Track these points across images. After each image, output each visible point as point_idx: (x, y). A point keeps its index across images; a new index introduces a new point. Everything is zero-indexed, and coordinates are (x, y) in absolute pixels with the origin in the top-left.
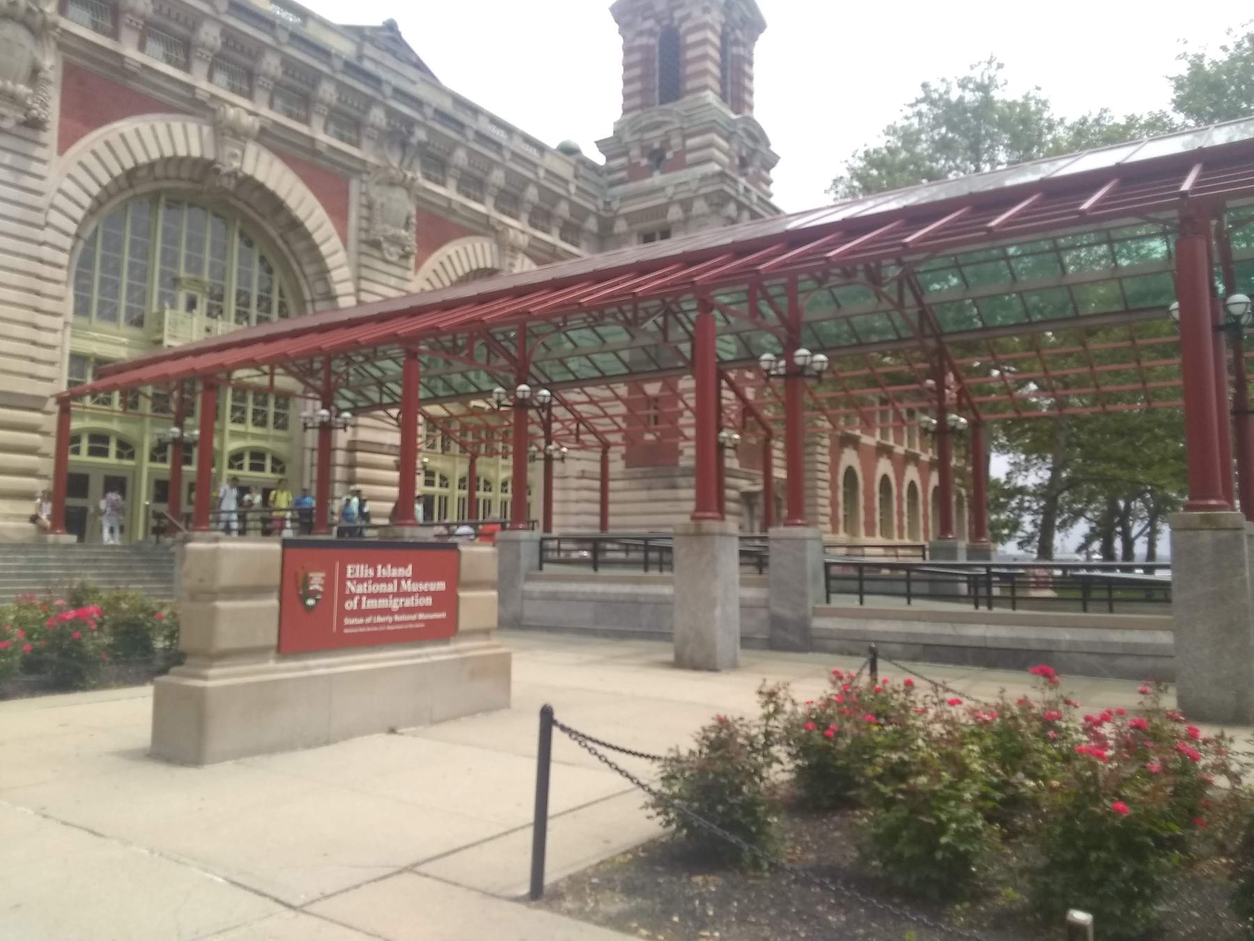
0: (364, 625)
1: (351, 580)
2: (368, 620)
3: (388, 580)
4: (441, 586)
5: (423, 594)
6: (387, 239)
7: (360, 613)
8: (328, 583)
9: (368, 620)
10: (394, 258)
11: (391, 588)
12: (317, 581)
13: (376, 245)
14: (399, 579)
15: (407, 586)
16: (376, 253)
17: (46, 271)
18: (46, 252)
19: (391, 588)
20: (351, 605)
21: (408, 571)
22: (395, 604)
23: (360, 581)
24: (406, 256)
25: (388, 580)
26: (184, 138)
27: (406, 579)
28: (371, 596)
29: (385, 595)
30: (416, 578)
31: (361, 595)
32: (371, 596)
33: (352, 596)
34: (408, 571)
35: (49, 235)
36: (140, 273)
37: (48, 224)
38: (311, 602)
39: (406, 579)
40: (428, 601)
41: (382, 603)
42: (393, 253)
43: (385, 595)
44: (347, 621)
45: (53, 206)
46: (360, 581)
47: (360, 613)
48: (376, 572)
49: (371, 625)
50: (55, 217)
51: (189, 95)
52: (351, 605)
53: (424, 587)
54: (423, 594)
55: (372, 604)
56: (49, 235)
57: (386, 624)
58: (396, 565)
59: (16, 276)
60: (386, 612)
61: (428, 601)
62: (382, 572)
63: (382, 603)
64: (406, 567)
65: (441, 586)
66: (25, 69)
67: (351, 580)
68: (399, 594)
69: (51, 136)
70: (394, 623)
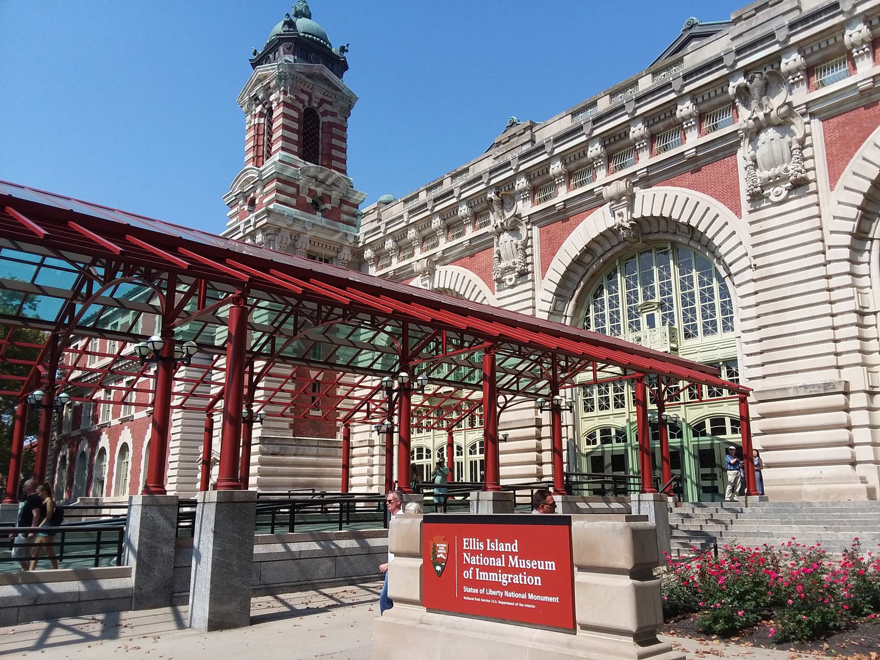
0: (478, 595)
1: (467, 551)
2: (482, 591)
3: (497, 554)
4: (551, 565)
5: (531, 572)
7: (474, 583)
8: (449, 550)
9: (482, 591)
11: (500, 563)
12: (442, 550)
14: (507, 554)
15: (514, 562)
19: (500, 563)
20: (468, 574)
21: (515, 547)
22: (504, 579)
23: (474, 553)
25: (497, 554)
27: (514, 554)
28: (483, 568)
29: (494, 569)
30: (522, 555)
31: (475, 566)
32: (483, 568)
33: (468, 566)
34: (515, 547)
38: (438, 568)
39: (514, 554)
40: (537, 581)
41: (493, 577)
43: (494, 569)
44: (467, 589)
46: (474, 553)
47: (474, 583)
48: (485, 546)
49: (485, 596)
52: (468, 574)
53: (532, 564)
54: (531, 572)
55: (483, 576)
57: (497, 597)
58: (502, 540)
60: (497, 586)
61: (537, 581)
62: (492, 546)
63: (493, 577)
64: (512, 543)
65: (551, 565)
67: (467, 551)
68: (507, 569)
70: (505, 598)
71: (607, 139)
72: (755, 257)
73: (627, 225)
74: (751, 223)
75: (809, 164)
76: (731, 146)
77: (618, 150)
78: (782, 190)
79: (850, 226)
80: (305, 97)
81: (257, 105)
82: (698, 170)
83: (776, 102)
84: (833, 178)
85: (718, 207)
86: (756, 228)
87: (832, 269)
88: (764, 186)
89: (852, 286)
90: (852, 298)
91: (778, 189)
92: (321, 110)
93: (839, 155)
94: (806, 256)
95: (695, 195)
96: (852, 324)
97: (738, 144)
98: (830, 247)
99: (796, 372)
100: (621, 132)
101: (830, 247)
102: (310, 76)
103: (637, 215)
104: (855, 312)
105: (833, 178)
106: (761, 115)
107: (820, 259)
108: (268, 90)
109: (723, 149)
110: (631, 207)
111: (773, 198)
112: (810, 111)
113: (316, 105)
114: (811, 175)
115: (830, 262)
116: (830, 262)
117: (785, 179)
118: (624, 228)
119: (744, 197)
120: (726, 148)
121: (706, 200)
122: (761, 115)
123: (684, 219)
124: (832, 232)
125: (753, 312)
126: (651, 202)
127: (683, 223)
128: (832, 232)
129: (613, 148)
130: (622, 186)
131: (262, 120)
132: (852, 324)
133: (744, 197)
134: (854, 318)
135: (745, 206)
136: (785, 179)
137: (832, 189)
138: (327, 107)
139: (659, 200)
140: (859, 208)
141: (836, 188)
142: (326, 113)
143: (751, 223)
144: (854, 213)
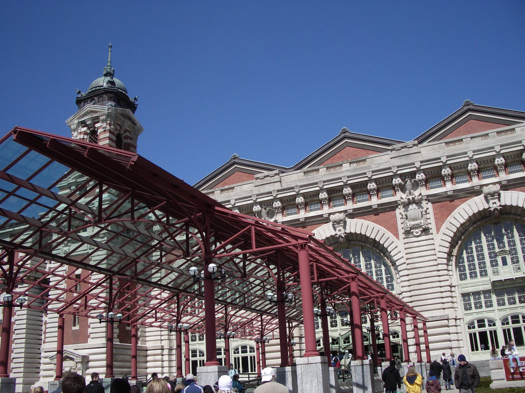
71: (330, 191)
72: (407, 259)
73: (343, 236)
74: (405, 244)
75: (429, 221)
76: (393, 207)
77: (335, 197)
78: (418, 231)
79: (447, 250)
80: (118, 128)
81: (83, 127)
82: (378, 214)
83: (416, 193)
84: (438, 230)
85: (388, 234)
86: (407, 246)
87: (440, 267)
88: (411, 228)
89: (447, 275)
90: (448, 280)
91: (417, 230)
92: (124, 135)
93: (440, 220)
94: (429, 261)
95: (377, 227)
96: (448, 291)
97: (397, 207)
98: (438, 258)
99: (427, 311)
100: (340, 189)
101: (438, 258)
102: (122, 115)
103: (348, 231)
104: (449, 286)
105: (438, 230)
106: (411, 197)
107: (435, 263)
108: (96, 120)
109: (390, 207)
110: (345, 227)
111: (414, 233)
112: (430, 198)
113: (122, 132)
114: (430, 226)
115: (439, 264)
116: (439, 264)
117: (421, 227)
118: (342, 237)
119: (401, 232)
120: (392, 207)
121: (383, 230)
122: (411, 197)
123: (373, 237)
124: (439, 252)
125: (407, 283)
126: (356, 226)
127: (372, 239)
128: (439, 252)
129: (333, 195)
130: (342, 216)
131: (86, 137)
132: (448, 291)
133: (401, 232)
134: (448, 288)
135: (402, 236)
136: (421, 227)
137: (438, 233)
138: (128, 134)
139: (358, 227)
140: (449, 243)
141: (440, 232)
142: (127, 137)
143: (405, 244)
144: (448, 245)
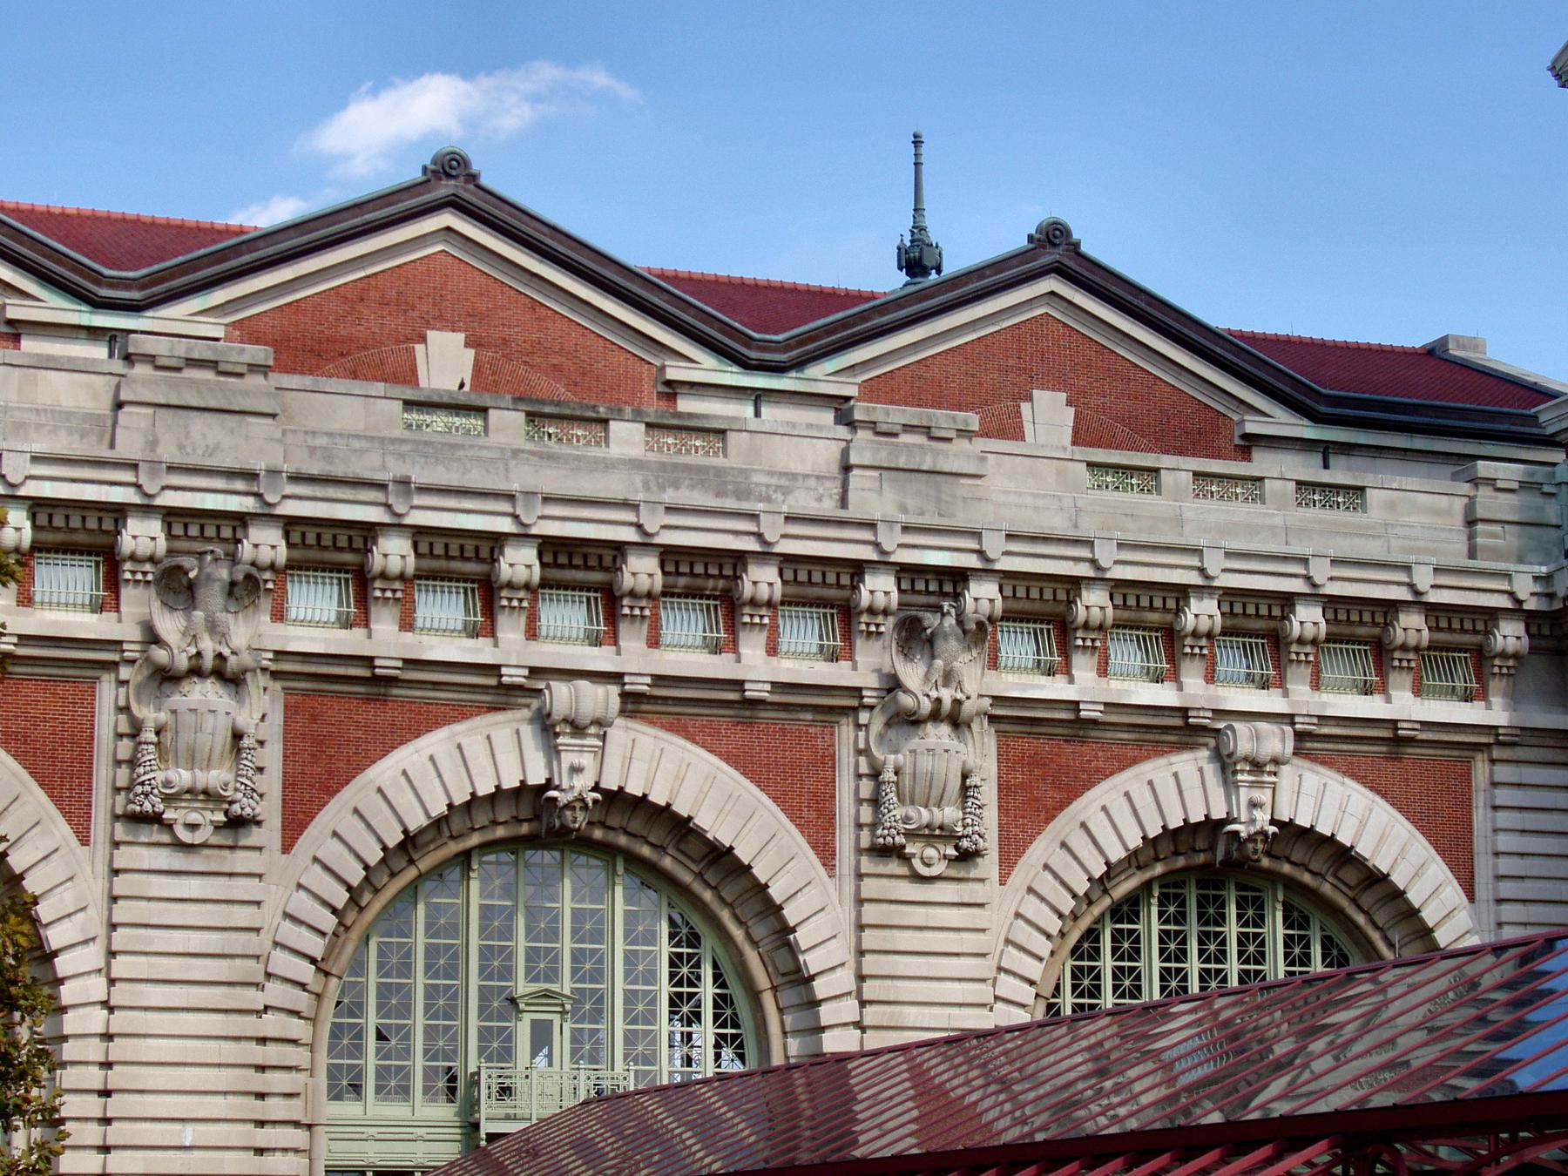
6: (911, 835)
10: (939, 868)
13: (884, 852)
16: (894, 867)
17: (272, 1054)
18: (272, 1024)
24: (967, 857)
26: (487, 755)
35: (276, 993)
36: (444, 1004)
37: (268, 975)
42: (933, 858)
45: (276, 944)
50: (284, 963)
51: (493, 681)
56: (276, 993)
59: (224, 1072)
66: (223, 738)
69: (269, 833)
